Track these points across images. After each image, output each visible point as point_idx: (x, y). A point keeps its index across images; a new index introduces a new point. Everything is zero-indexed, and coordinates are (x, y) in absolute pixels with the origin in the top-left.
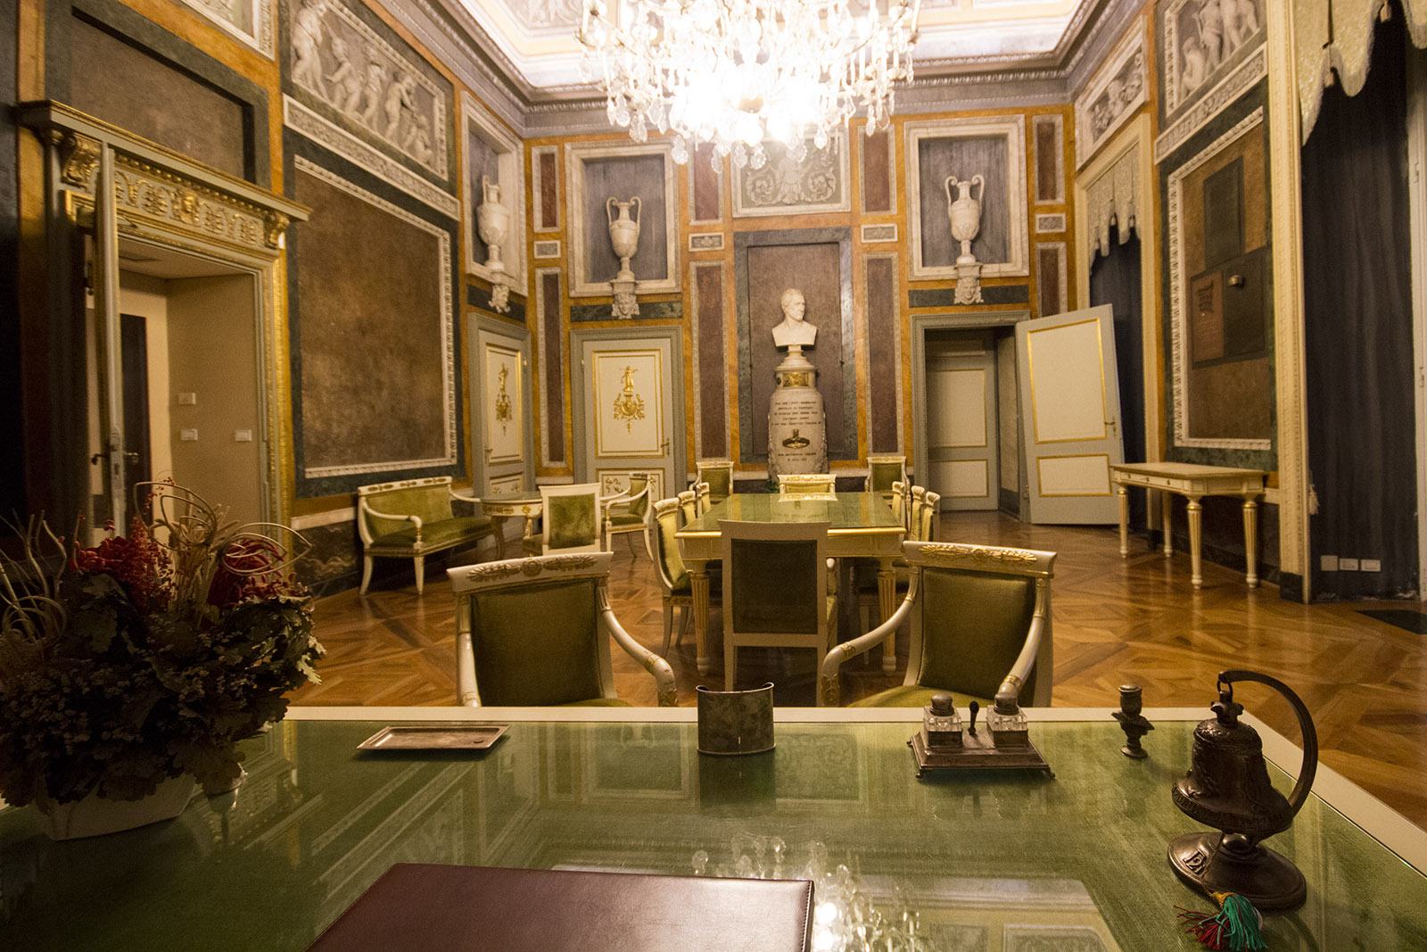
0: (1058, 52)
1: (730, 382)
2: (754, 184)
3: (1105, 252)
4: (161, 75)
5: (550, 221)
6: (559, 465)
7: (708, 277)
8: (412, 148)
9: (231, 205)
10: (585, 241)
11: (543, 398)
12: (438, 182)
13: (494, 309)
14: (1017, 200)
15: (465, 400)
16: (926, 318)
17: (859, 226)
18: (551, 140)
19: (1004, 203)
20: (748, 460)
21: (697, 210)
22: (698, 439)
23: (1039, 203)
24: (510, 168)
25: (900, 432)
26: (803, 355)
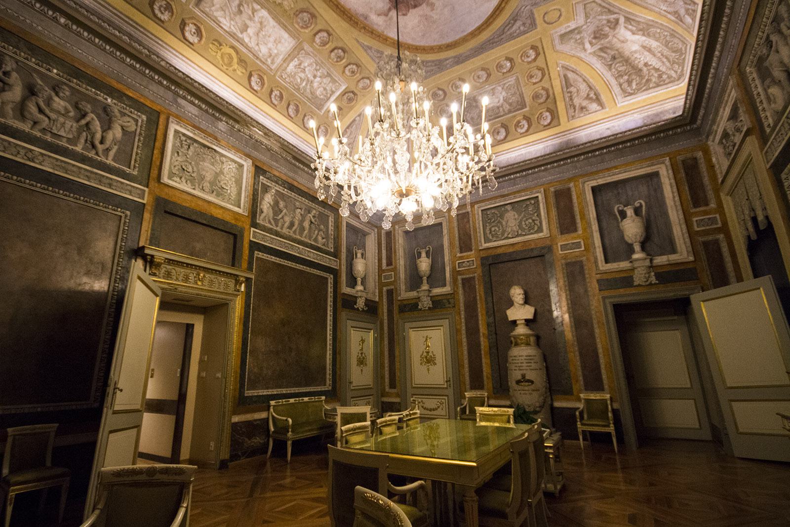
0: (685, 114)
2: (490, 230)
3: (754, 237)
4: (200, 228)
6: (393, 391)
7: (468, 283)
8: (316, 240)
9: (220, 276)
11: (386, 353)
13: (358, 309)
14: (675, 212)
16: (611, 297)
17: (557, 244)
25: (604, 377)
26: (527, 325)
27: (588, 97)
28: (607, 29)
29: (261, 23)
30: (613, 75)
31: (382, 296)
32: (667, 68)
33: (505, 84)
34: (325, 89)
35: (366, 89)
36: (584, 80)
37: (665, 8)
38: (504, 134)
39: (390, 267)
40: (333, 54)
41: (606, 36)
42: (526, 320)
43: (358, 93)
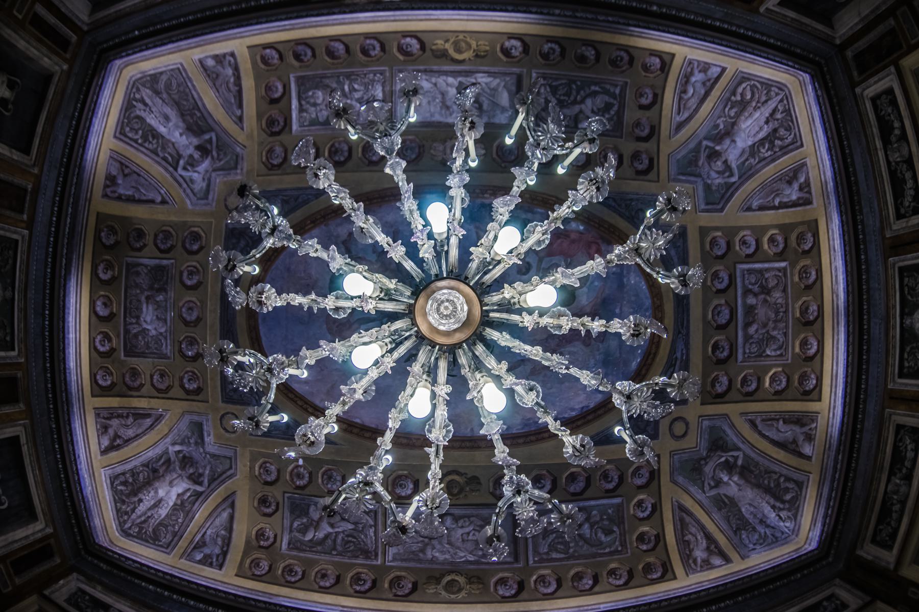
27: (117, 436)
29: (448, 108)
30: (136, 467)
33: (166, 338)
34: (315, 105)
35: (268, 152)
36: (137, 436)
38: (101, 313)
40: (346, 148)
43: (271, 139)
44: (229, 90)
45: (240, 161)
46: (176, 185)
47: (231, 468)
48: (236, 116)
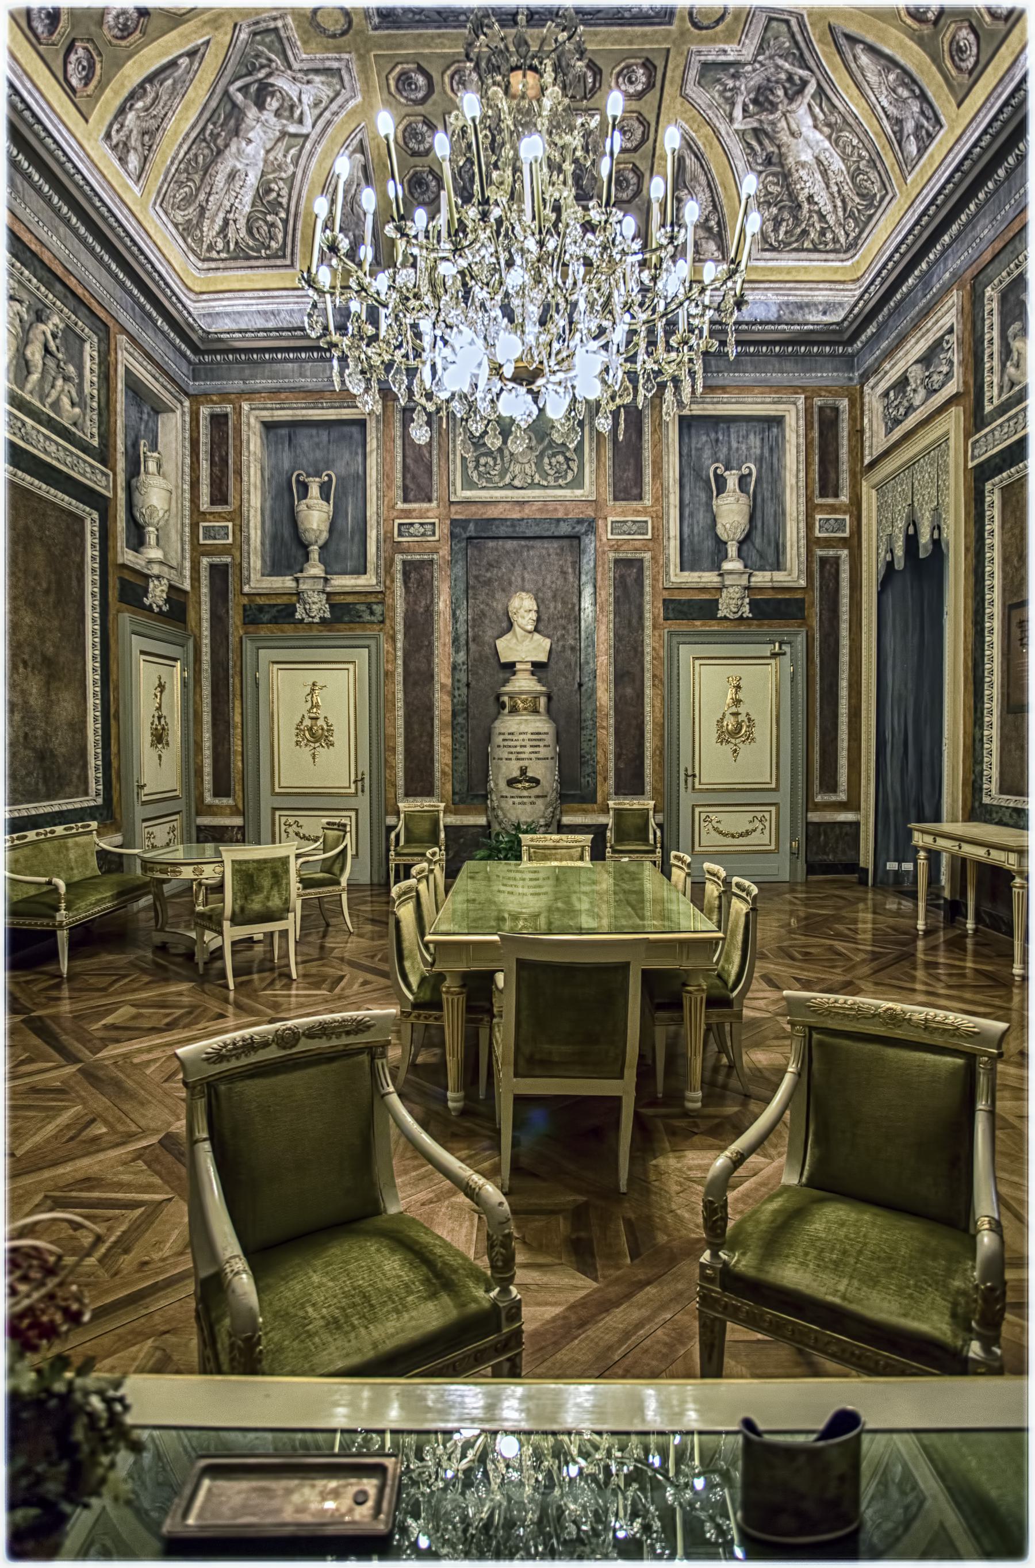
1: (442, 705)
3: (899, 565)
5: (219, 496)
6: (225, 801)
10: (263, 523)
11: (207, 718)
12: (86, 448)
15: (113, 722)
18: (225, 397)
19: (778, 498)
20: (462, 801)
21: (405, 489)
22: (401, 774)
23: (818, 501)
24: (172, 430)
25: (648, 771)
26: (533, 674)
28: (780, 93)
31: (199, 580)
32: (838, 220)
37: (885, 104)
39: (218, 509)
41: (773, 107)
42: (534, 664)
44: (157, 97)
45: (263, 25)
46: (330, 130)
47: (787, 22)
48: (191, 63)
